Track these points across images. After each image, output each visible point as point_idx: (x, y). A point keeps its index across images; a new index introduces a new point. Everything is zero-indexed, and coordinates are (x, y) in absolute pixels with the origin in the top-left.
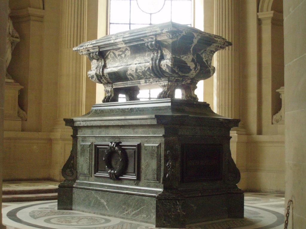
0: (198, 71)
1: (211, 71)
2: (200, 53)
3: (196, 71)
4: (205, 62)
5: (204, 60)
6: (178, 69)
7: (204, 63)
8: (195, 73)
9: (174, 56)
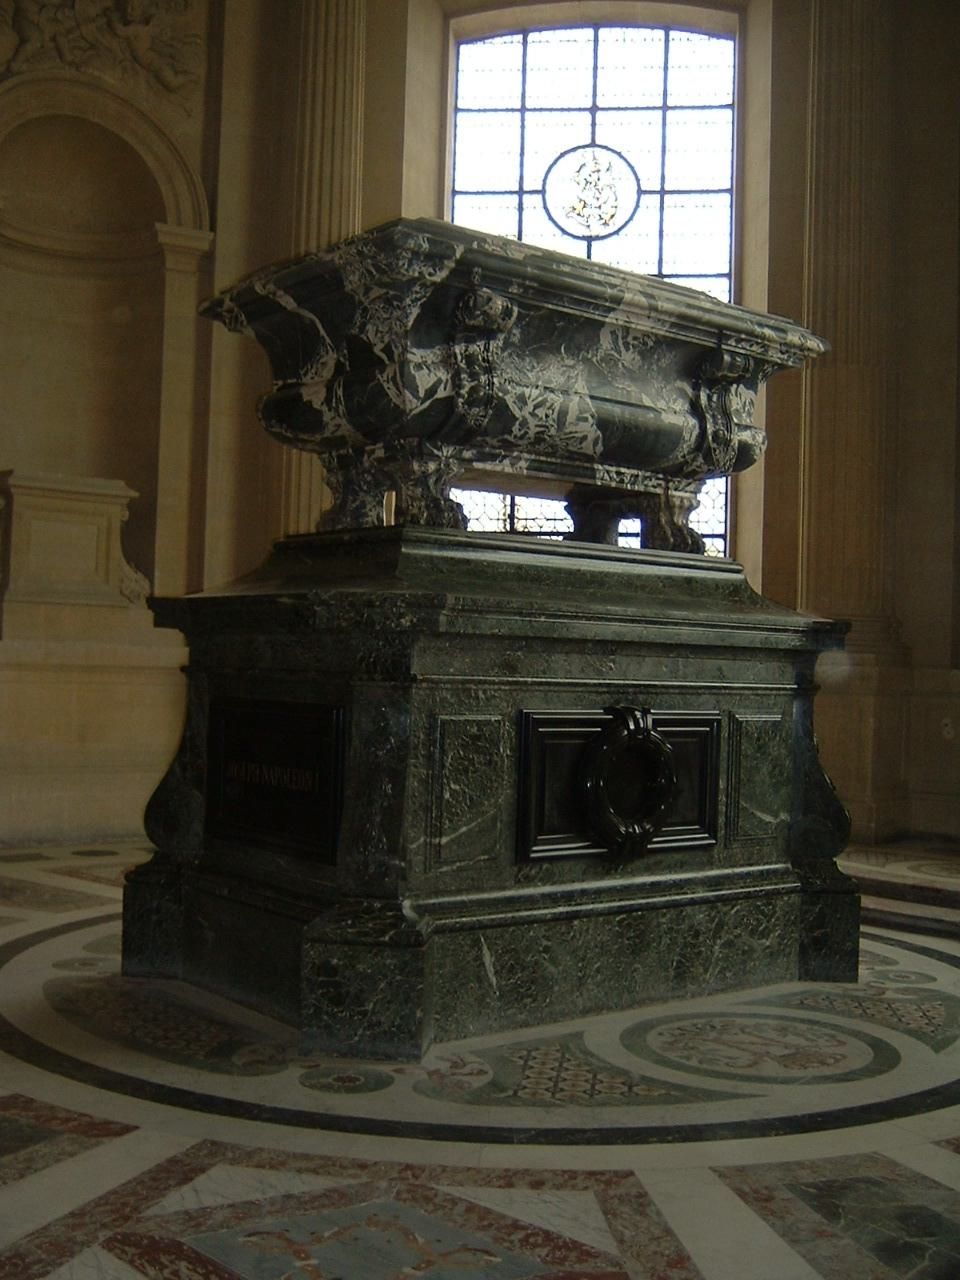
1: (385, 385)
2: (356, 331)
3: (337, 410)
4: (384, 356)
5: (377, 350)
7: (379, 358)
8: (339, 416)
9: (280, 383)
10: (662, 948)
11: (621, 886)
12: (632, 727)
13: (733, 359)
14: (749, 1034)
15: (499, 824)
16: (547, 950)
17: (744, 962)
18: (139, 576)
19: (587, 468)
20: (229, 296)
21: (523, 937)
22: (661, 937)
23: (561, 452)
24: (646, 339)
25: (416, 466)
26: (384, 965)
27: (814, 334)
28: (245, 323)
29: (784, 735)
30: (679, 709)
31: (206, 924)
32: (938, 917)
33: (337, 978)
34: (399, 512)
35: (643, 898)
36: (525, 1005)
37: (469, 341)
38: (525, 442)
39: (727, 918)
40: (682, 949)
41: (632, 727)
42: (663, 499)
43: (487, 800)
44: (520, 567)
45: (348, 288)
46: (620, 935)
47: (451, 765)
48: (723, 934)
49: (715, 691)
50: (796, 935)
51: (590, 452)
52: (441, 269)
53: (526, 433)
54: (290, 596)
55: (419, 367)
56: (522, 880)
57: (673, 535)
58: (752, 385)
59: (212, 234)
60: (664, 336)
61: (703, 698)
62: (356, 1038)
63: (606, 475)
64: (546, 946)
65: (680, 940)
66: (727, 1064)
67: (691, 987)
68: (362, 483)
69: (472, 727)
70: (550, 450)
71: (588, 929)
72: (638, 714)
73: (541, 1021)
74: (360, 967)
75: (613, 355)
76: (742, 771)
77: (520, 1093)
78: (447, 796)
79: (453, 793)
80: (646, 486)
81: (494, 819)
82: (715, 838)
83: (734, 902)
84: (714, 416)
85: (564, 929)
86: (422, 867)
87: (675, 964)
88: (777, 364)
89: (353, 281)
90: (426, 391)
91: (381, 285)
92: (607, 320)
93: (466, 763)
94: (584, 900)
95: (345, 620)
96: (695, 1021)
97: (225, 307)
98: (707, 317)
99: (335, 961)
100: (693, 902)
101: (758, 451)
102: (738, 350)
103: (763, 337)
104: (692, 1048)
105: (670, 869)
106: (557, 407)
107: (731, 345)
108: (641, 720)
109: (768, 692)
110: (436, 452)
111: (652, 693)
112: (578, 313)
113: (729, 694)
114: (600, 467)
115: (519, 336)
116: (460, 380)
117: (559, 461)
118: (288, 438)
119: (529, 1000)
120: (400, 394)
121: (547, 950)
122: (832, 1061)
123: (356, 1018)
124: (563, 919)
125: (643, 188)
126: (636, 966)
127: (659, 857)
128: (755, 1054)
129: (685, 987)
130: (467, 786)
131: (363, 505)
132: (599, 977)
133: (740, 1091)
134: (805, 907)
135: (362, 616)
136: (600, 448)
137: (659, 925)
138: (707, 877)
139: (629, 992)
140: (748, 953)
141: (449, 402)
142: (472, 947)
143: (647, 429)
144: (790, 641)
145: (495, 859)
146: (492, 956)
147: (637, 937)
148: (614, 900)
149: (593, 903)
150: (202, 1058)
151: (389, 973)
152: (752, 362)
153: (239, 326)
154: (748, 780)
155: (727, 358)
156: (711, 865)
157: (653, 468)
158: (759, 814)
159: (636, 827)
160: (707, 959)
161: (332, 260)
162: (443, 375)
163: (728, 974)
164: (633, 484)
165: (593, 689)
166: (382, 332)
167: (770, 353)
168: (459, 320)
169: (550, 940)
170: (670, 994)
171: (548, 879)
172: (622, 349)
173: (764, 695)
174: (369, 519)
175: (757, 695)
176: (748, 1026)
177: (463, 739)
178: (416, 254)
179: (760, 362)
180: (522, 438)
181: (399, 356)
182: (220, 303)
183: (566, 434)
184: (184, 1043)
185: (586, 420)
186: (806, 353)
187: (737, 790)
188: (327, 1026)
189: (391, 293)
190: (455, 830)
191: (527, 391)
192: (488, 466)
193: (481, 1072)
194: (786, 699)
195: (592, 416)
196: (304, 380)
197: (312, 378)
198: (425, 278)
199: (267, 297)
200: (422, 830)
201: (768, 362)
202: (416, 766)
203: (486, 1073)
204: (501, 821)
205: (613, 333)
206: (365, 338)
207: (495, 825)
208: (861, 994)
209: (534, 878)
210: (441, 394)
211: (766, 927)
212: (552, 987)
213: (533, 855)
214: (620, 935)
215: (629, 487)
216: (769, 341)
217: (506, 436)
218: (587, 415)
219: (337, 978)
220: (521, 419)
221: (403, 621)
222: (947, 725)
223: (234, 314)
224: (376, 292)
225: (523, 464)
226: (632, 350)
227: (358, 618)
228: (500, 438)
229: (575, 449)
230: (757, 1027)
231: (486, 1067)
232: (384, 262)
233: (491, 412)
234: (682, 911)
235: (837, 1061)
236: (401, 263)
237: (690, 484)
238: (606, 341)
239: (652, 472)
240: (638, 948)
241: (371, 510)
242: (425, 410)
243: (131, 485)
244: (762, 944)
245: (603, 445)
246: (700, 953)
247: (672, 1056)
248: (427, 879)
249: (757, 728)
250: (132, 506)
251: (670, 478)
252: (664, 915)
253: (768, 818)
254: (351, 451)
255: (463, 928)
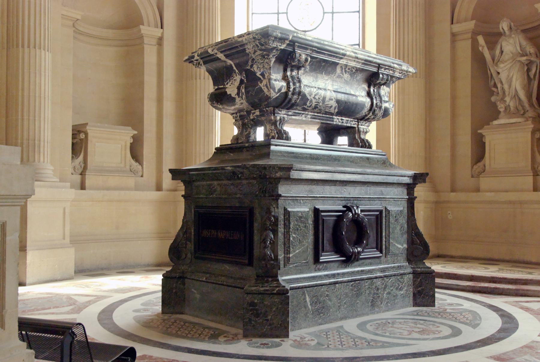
0: (243, 96)
1: (263, 88)
2: (249, 68)
3: (242, 97)
5: (258, 74)
6: (219, 103)
7: (259, 77)
9: (216, 87)
10: (366, 295)
11: (351, 271)
12: (354, 212)
13: (383, 76)
14: (403, 324)
15: (309, 249)
16: (327, 295)
17: (395, 300)
18: (137, 164)
19: (331, 118)
20: (197, 54)
21: (319, 291)
22: (366, 291)
23: (323, 112)
24: (353, 69)
25: (272, 118)
26: (274, 301)
27: (412, 66)
28: (203, 65)
29: (404, 215)
30: (368, 205)
31: (195, 292)
32: (457, 284)
33: (257, 307)
34: (266, 135)
35: (359, 276)
36: (321, 317)
37: (292, 71)
38: (311, 108)
39: (388, 284)
40: (373, 295)
41: (354, 212)
42: (357, 128)
43: (305, 240)
44: (311, 154)
45: (247, 51)
46: (352, 290)
47: (292, 227)
48: (387, 289)
49: (380, 199)
50: (412, 290)
51: (333, 112)
52: (284, 44)
53: (312, 105)
54: (231, 167)
55: (275, 80)
56: (317, 270)
57: (361, 142)
58: (388, 86)
59: (162, 30)
60: (359, 68)
61: (376, 202)
62: (265, 330)
63: (337, 121)
64: (327, 294)
65: (372, 292)
66: (400, 334)
67: (377, 309)
68: (249, 125)
69: (299, 213)
70: (319, 111)
71: (341, 288)
72: (355, 208)
73: (326, 323)
74: (266, 303)
75: (340, 75)
76: (390, 229)
77: (330, 346)
78: (291, 239)
79: (294, 238)
80: (351, 124)
81: (307, 247)
82: (382, 254)
83: (390, 277)
84: (376, 98)
85: (333, 288)
86: (283, 265)
87: (371, 301)
88: (398, 78)
89: (249, 49)
90: (278, 89)
91: (261, 50)
92: (340, 62)
93: (298, 227)
94: (339, 277)
95: (255, 174)
96: (382, 321)
97: (195, 59)
98: (375, 60)
99: (256, 301)
100: (376, 278)
101: (391, 110)
102: (384, 72)
103: (394, 68)
104: (385, 330)
105: (367, 265)
106: (322, 95)
107: (382, 71)
108: (356, 210)
109: (398, 199)
110: (280, 112)
111: (359, 200)
112: (330, 59)
113: (385, 200)
114: (335, 117)
115: (309, 68)
116: (290, 85)
117: (321, 115)
118: (220, 108)
119: (322, 315)
120: (269, 91)
121: (327, 295)
122: (437, 333)
123: (264, 322)
124: (332, 284)
125: (325, 11)
126: (358, 301)
127: (363, 261)
128: (409, 331)
129: (374, 309)
130: (298, 235)
131: (249, 133)
132: (345, 306)
133: (408, 343)
134: (414, 279)
135: (262, 173)
136: (336, 110)
137: (365, 286)
138: (380, 268)
139: (356, 311)
140: (395, 296)
141: (286, 94)
142: (302, 295)
143: (353, 103)
144: (407, 180)
145: (308, 262)
146: (309, 298)
147: (358, 291)
148: (349, 277)
149: (342, 278)
150: (207, 339)
151: (277, 305)
152: (389, 77)
153: (200, 66)
154: (393, 232)
155: (381, 76)
156: (380, 263)
157: (354, 117)
158: (396, 245)
159: (356, 250)
160: (382, 299)
161: (242, 40)
162: (284, 84)
163: (389, 305)
164: (347, 123)
165: (339, 199)
166: (260, 68)
167: (395, 74)
168: (289, 63)
169: (328, 292)
170: (369, 312)
171: (325, 269)
172: (344, 73)
173: (397, 200)
174: (252, 138)
175: (395, 200)
176: (401, 322)
177: (296, 218)
178: (276, 38)
179: (392, 77)
180: (310, 107)
181: (267, 76)
182: (193, 57)
183: (325, 105)
184: (198, 335)
185: (332, 100)
186: (408, 73)
187: (389, 236)
188: (254, 326)
189: (265, 53)
190: (294, 251)
191: (312, 89)
192: (297, 118)
193: (312, 340)
194: (404, 202)
195: (335, 99)
196: (227, 86)
197: (230, 85)
198: (278, 47)
199: (213, 55)
200: (283, 252)
201: (394, 77)
202: (280, 228)
203: (314, 340)
204: (310, 248)
205: (341, 67)
206: (253, 70)
207: (307, 250)
208: (438, 311)
209: (321, 269)
210: (284, 90)
211: (401, 287)
212: (329, 310)
213: (321, 261)
214: (352, 290)
215: (345, 125)
216: (396, 69)
217: (305, 106)
218: (333, 98)
219: (257, 307)
220: (310, 100)
221: (277, 174)
222: (449, 214)
223: (198, 61)
224: (259, 52)
225: (309, 116)
226: (347, 73)
227: (260, 174)
228: (302, 107)
229: (328, 111)
230: (405, 322)
231: (313, 338)
232: (264, 41)
233: (300, 97)
234: (372, 281)
235: (439, 332)
236: (270, 42)
237: (366, 123)
238: (338, 70)
239: (353, 119)
240: (358, 295)
241: (252, 135)
242: (277, 97)
243: (134, 129)
244: (400, 293)
245: (338, 109)
246: (379, 296)
247: (377, 332)
248: (285, 270)
249: (395, 213)
250: (133, 137)
251: (359, 121)
252: (367, 282)
253: (400, 246)
254: (245, 113)
255: (299, 288)
